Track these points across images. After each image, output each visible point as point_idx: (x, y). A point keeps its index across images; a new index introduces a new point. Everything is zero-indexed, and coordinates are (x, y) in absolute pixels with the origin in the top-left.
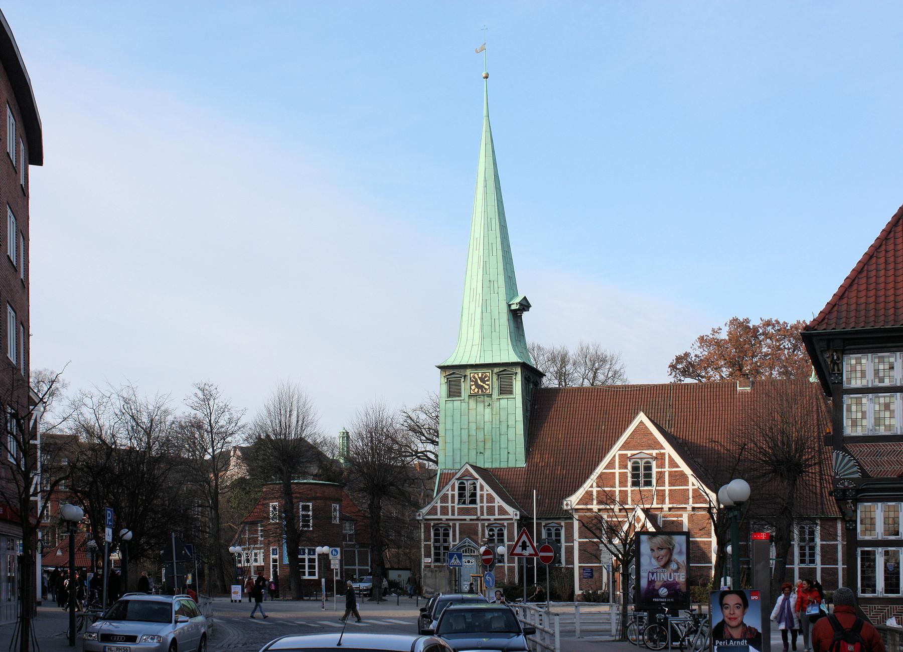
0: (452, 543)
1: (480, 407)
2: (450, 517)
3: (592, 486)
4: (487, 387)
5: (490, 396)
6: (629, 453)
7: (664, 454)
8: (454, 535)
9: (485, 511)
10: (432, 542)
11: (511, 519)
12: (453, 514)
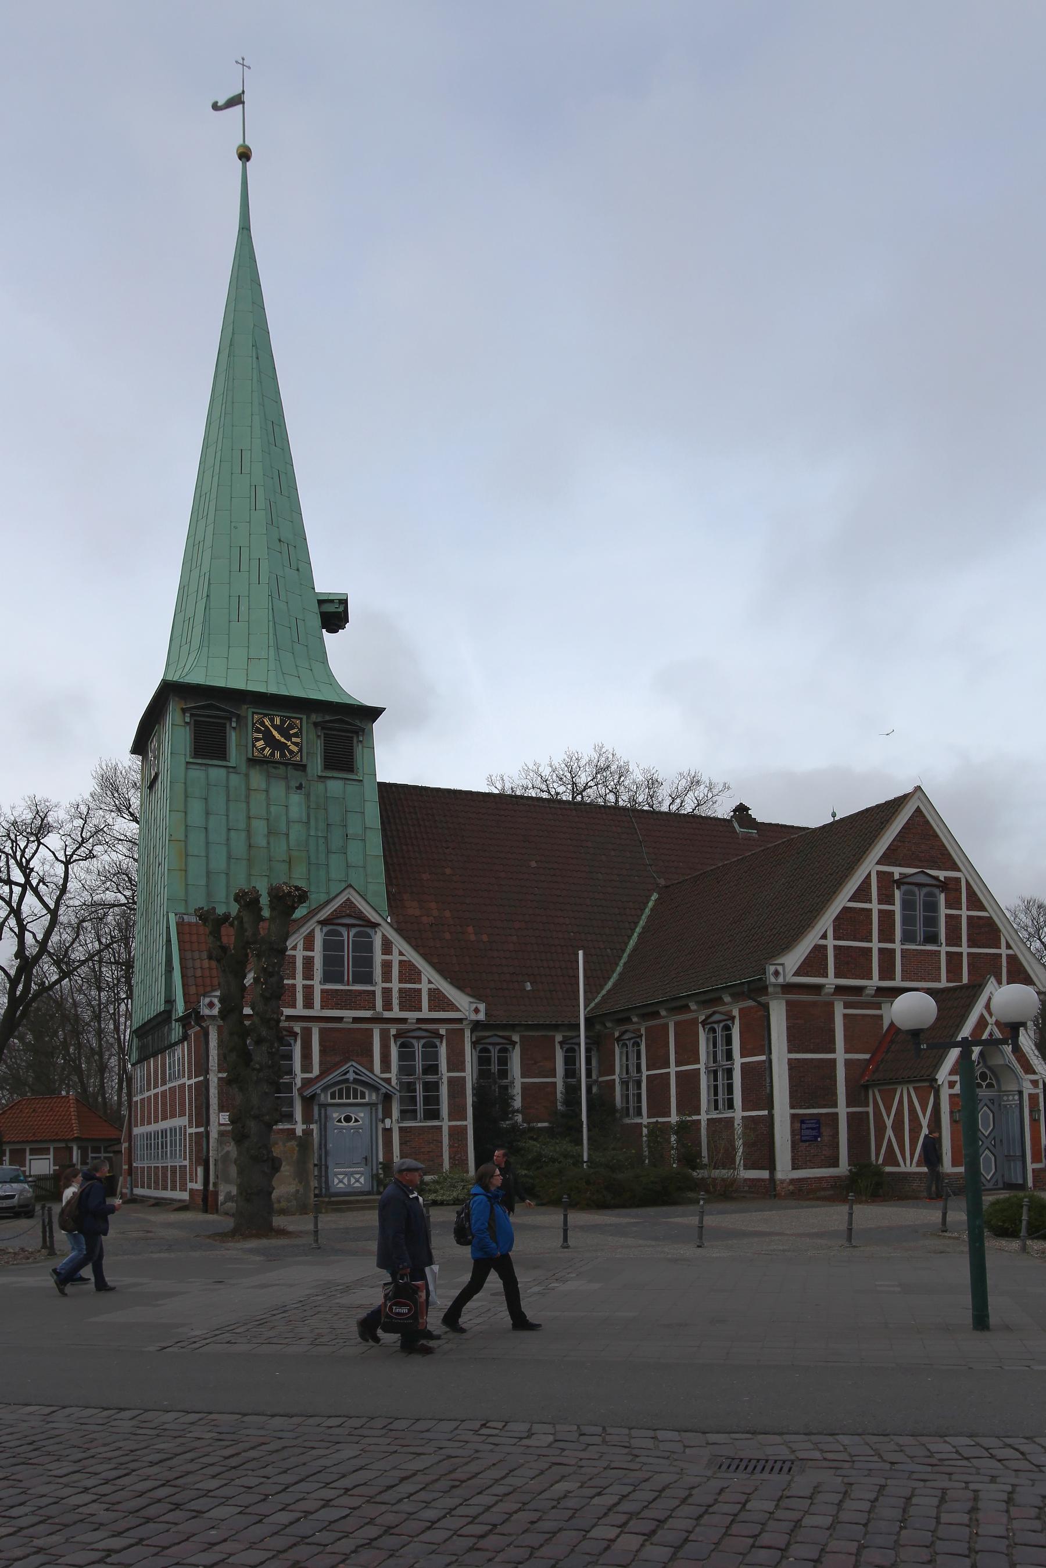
0: (299, 1076)
1: (278, 790)
5: (301, 767)
9: (395, 1002)
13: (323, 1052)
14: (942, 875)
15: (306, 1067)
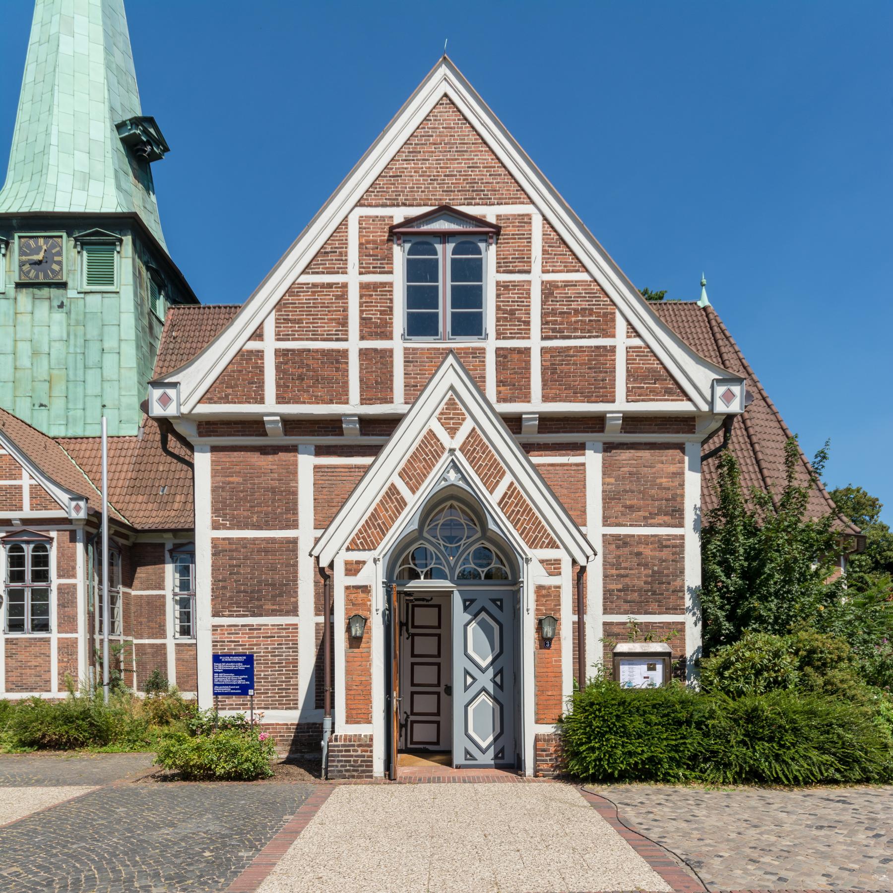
3: (258, 335)
6: (399, 215)
7: (525, 220)
14: (490, 213)
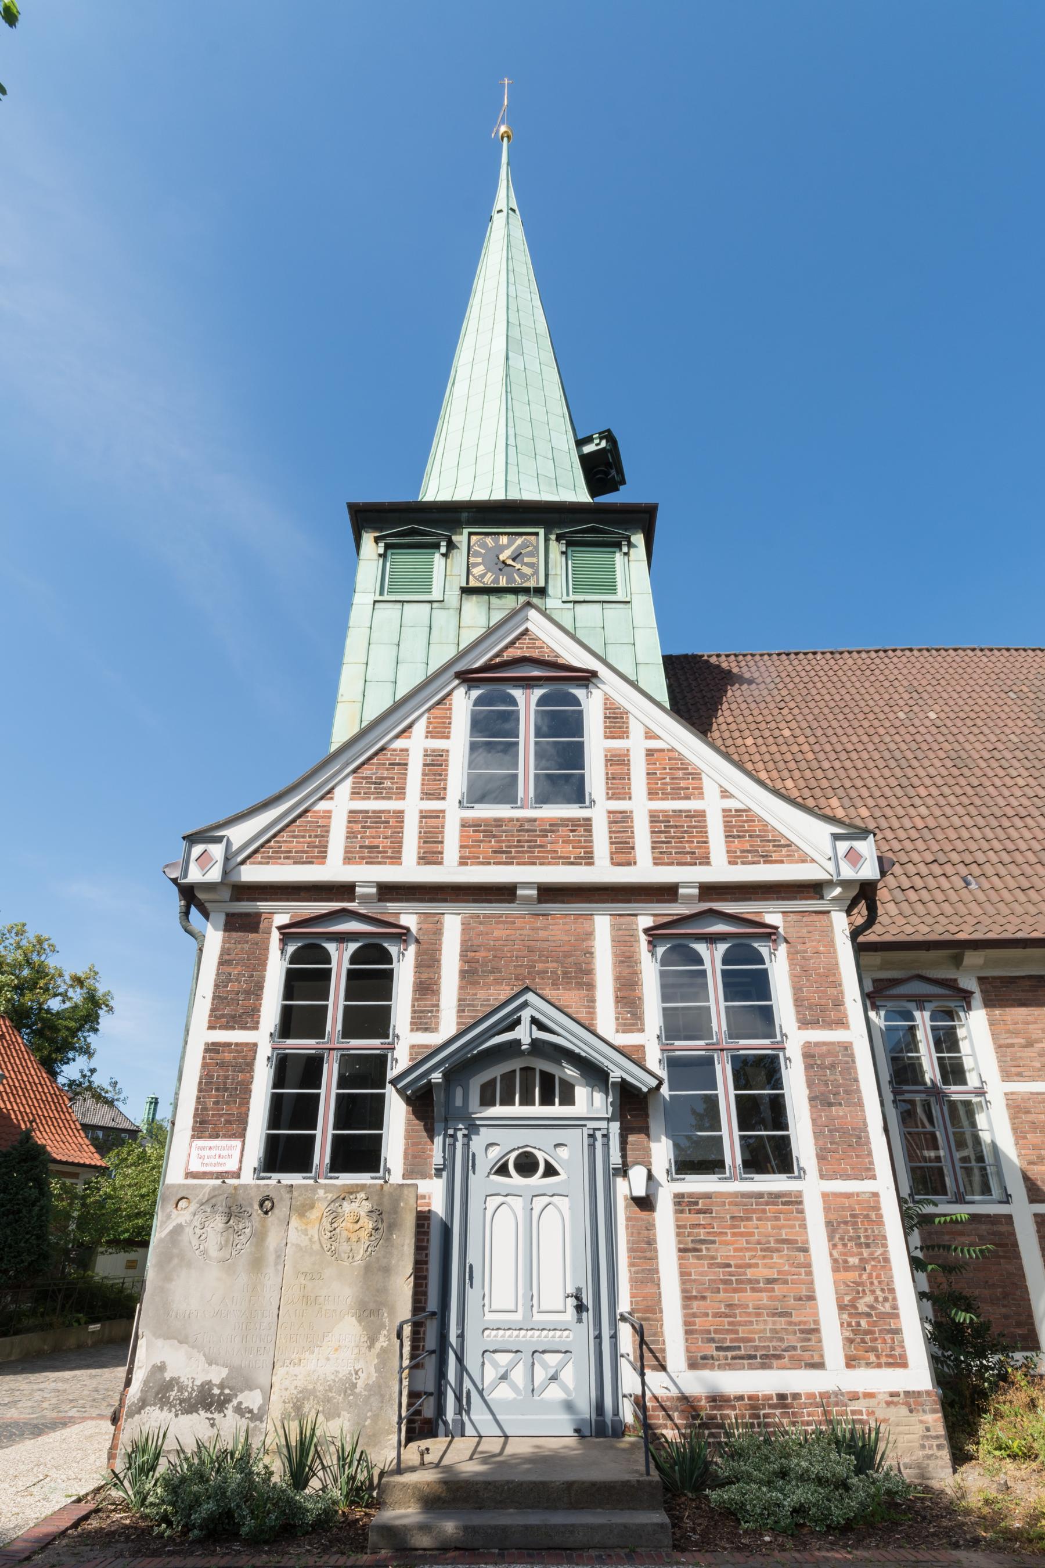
2: (409, 870)
4: (526, 570)
8: (426, 988)
10: (263, 1037)
11: (814, 889)
12: (430, 855)
13: (469, 975)
15: (422, 1021)
